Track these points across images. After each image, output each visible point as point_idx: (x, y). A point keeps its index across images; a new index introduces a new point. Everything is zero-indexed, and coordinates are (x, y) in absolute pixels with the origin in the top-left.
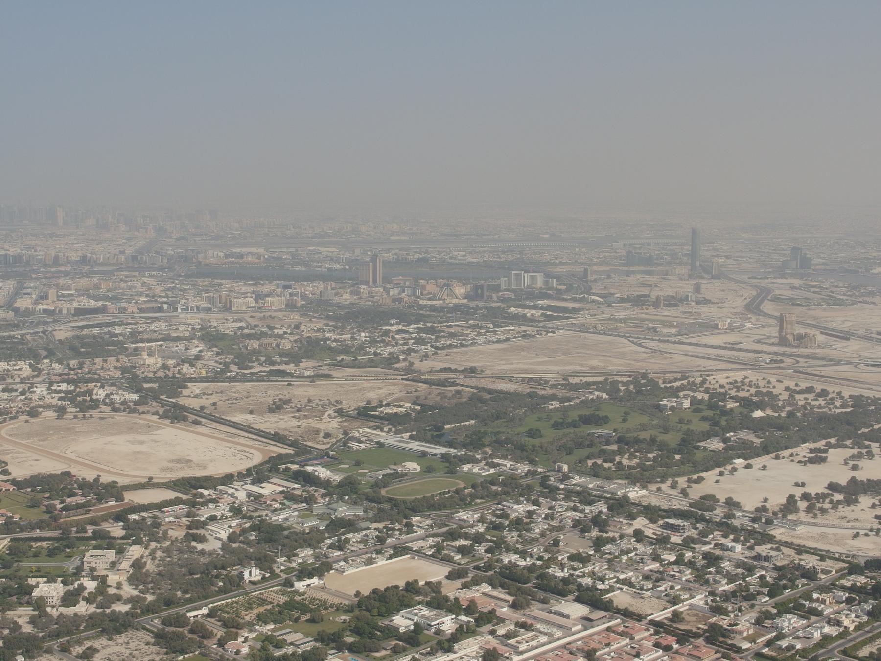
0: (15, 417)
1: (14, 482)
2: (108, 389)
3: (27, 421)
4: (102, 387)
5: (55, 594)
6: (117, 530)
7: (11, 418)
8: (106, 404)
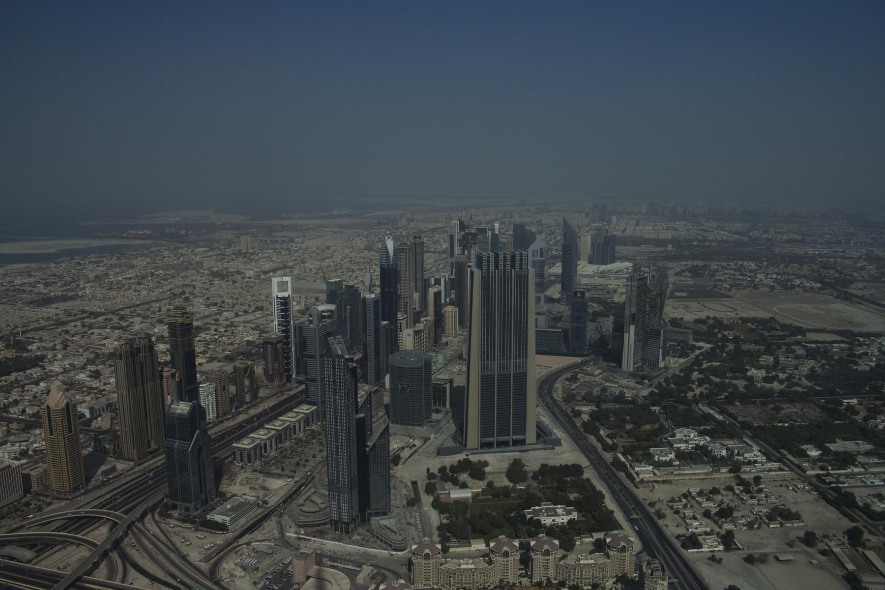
0: (745, 288)
1: (741, 319)
2: (802, 280)
3: (751, 291)
4: (798, 278)
5: (760, 375)
6: (800, 351)
7: (743, 289)
8: (800, 287)
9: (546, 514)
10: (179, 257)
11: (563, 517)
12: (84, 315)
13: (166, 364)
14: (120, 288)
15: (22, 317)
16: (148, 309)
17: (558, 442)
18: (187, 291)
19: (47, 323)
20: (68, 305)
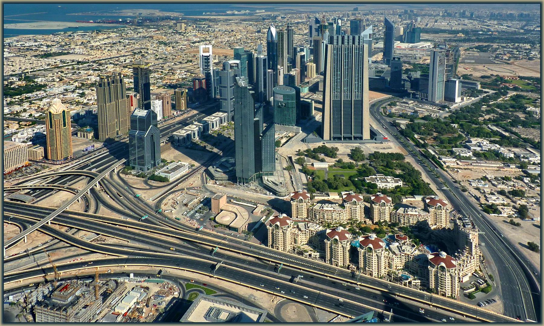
9: (380, 181)
10: (137, 34)
11: (392, 184)
12: (73, 63)
13: (129, 89)
14: (98, 49)
15: (30, 64)
16: (117, 61)
17: (385, 139)
18: (143, 52)
19: (49, 67)
20: (63, 57)
